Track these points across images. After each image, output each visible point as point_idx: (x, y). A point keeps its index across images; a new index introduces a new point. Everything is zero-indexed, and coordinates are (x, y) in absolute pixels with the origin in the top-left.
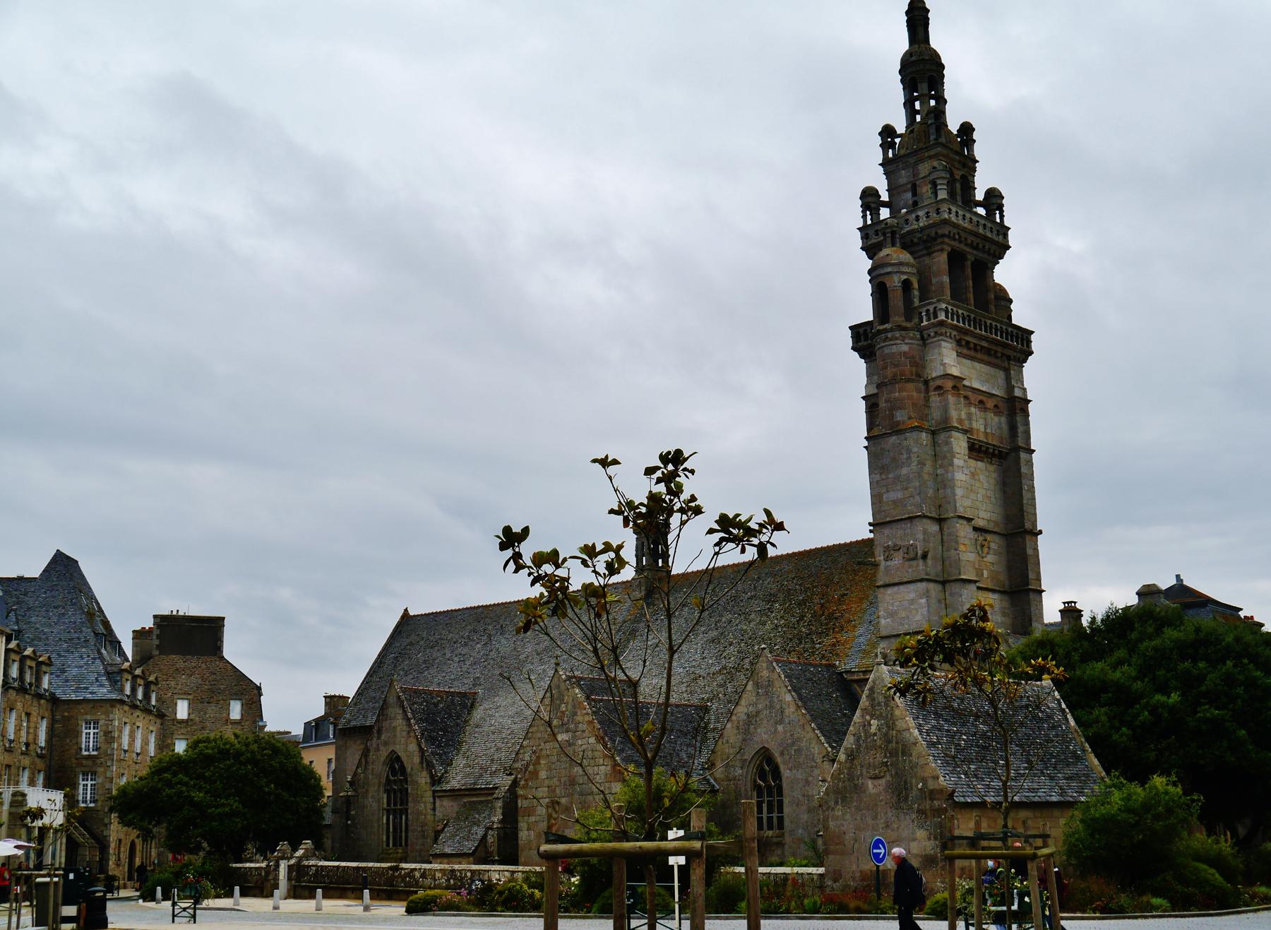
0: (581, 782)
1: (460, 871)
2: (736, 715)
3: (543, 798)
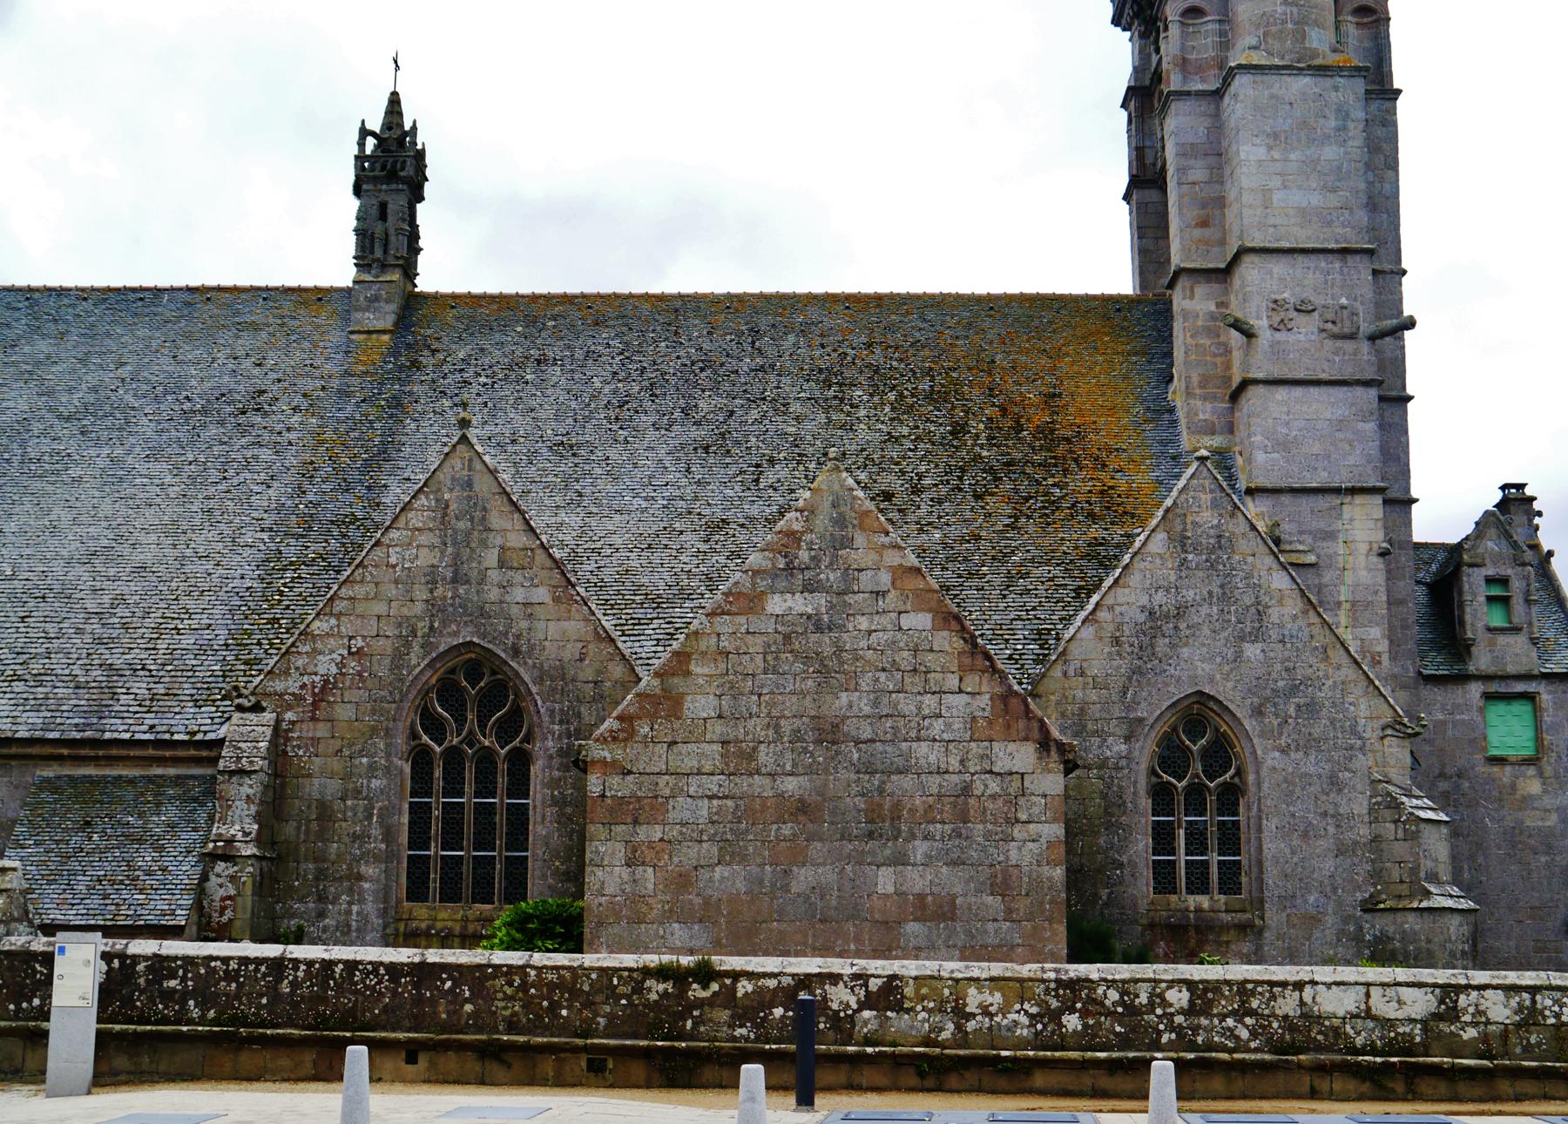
0: (867, 734)
1: (1124, 987)
2: (1111, 608)
3: (699, 773)
